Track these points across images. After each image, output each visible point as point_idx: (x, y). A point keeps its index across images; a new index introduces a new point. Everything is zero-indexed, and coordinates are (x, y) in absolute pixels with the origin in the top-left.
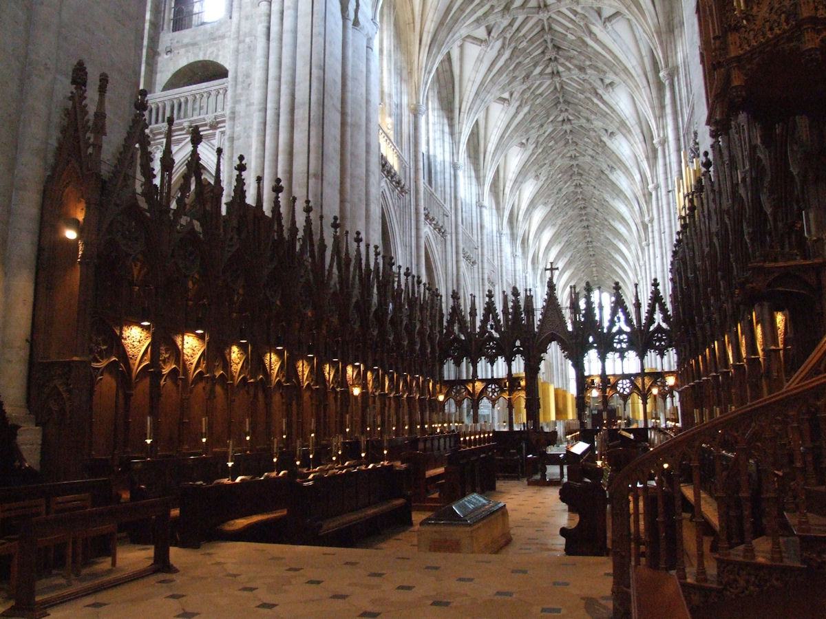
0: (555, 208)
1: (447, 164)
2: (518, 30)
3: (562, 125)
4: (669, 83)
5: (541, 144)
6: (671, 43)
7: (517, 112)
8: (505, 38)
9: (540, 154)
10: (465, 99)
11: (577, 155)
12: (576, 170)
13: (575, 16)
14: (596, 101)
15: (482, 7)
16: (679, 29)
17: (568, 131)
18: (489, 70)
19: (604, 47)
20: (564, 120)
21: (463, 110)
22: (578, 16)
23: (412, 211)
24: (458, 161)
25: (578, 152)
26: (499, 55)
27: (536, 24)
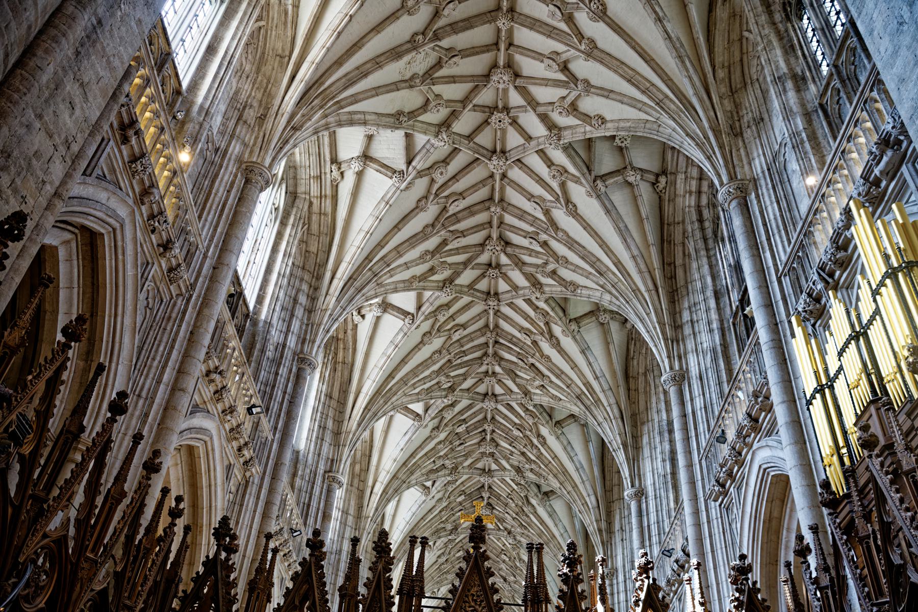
0: (443, 559)
1: (288, 354)
2: (455, 178)
3: (483, 401)
4: (739, 204)
5: (446, 425)
6: (738, 150)
7: (422, 342)
8: (433, 181)
9: (440, 443)
10: (347, 258)
11: (494, 467)
12: (486, 495)
13: (549, 167)
14: (545, 346)
15: (411, 87)
16: (754, 128)
17: (489, 417)
18: (395, 227)
19: (587, 227)
20: (486, 395)
21: (339, 275)
22: (553, 168)
23: (181, 334)
24: (311, 353)
25: (496, 461)
26: (417, 207)
27: (483, 182)
